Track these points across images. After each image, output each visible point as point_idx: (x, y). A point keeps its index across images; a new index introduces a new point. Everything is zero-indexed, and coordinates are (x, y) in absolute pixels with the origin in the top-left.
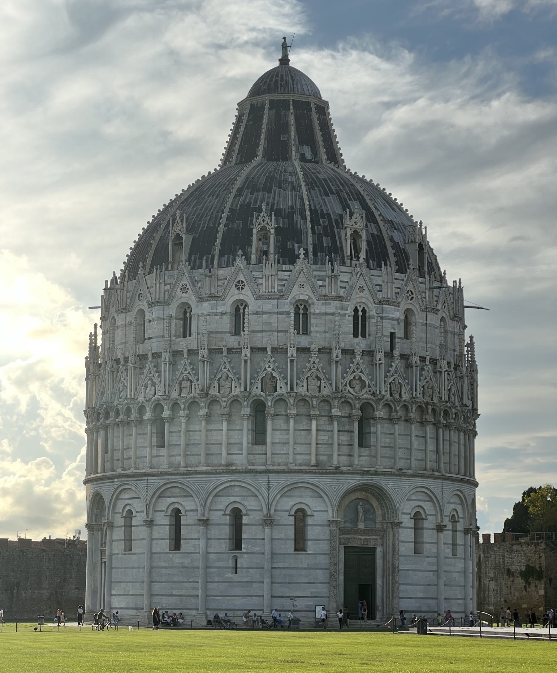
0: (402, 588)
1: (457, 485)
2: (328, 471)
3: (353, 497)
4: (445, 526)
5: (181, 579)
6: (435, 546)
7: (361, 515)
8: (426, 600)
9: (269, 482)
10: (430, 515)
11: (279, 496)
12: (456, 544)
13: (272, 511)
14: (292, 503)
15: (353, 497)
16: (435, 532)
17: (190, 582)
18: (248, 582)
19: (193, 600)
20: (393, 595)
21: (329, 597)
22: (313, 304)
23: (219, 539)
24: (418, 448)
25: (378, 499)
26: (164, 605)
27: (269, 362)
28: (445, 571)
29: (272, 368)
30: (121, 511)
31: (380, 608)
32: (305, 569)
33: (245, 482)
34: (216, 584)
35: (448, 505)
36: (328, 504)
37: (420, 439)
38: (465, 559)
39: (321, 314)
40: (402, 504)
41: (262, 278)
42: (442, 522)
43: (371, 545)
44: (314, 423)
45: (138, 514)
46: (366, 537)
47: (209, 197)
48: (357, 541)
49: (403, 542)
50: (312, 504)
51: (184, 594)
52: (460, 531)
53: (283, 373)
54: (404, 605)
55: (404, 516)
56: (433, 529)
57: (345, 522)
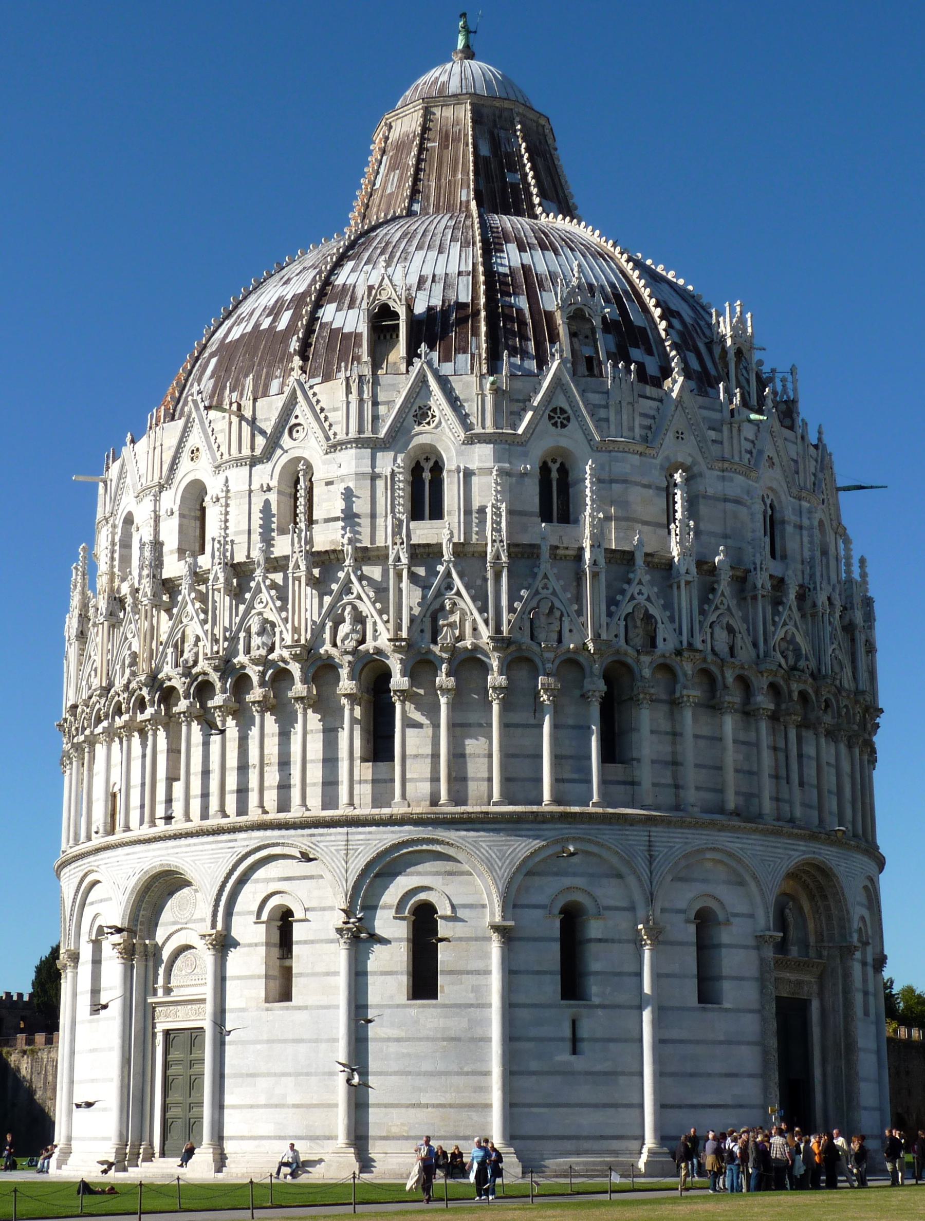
5: (441, 1067)
9: (650, 845)
14: (690, 895)
17: (467, 1074)
18: (606, 1074)
19: (475, 1116)
22: (701, 475)
23: (538, 973)
25: (812, 898)
26: (395, 1130)
27: (640, 583)
29: (645, 596)
30: (255, 908)
33: (598, 844)
34: (534, 1078)
36: (758, 899)
39: (715, 498)
41: (606, 406)
45: (309, 916)
47: (419, 247)
50: (732, 900)
51: (452, 1101)
53: (668, 606)
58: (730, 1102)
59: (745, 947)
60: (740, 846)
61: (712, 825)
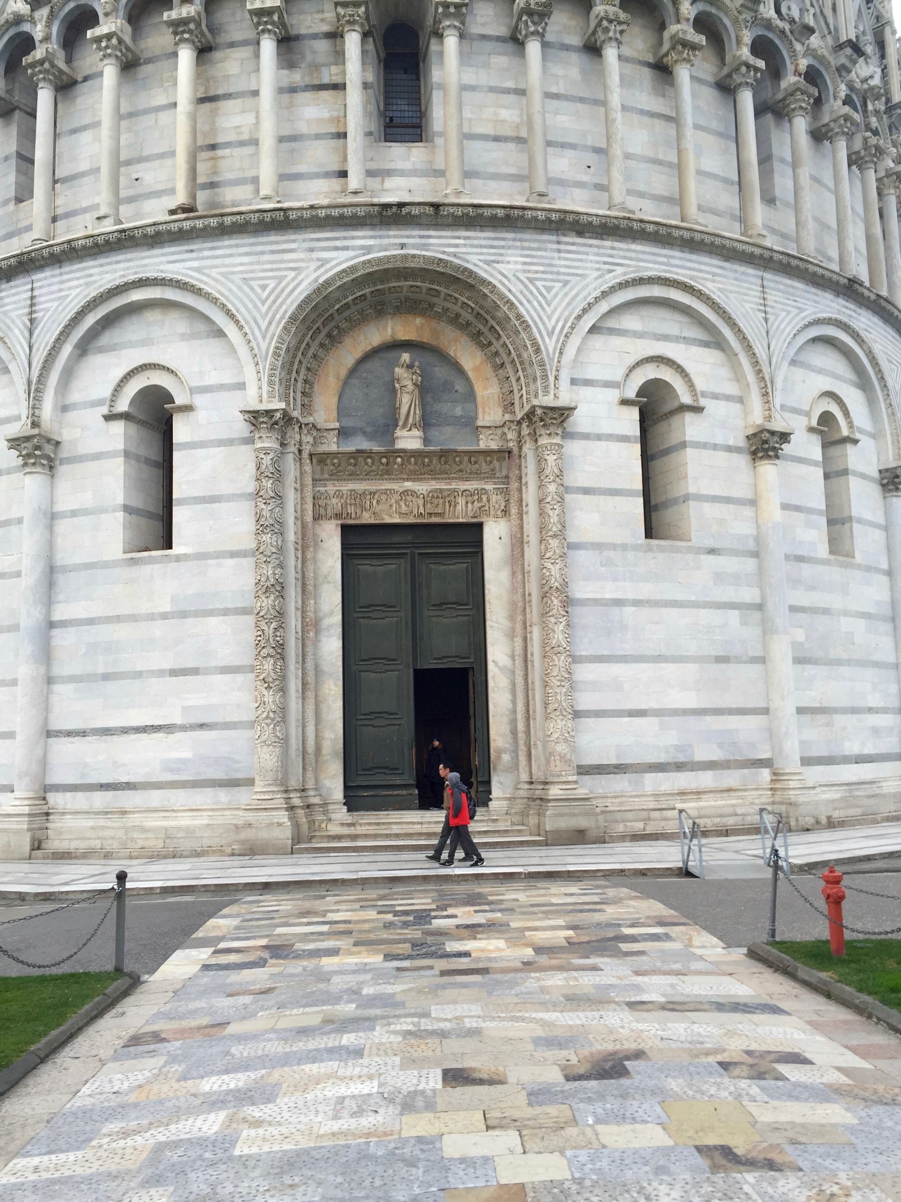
0: (585, 673)
1: (831, 306)
2: (228, 220)
3: (374, 335)
4: (785, 437)
6: (748, 512)
7: (406, 401)
8: (709, 719)
10: (715, 396)
11: (67, 349)
12: (850, 519)
13: (47, 410)
14: (118, 373)
15: (374, 335)
16: (742, 461)
20: (546, 705)
21: (251, 725)
24: (651, 154)
25: (476, 337)
28: (793, 609)
31: (506, 757)
32: (164, 616)
35: (799, 372)
36: (242, 350)
37: (659, 124)
38: (890, 573)
40: (575, 342)
42: (769, 418)
43: (461, 513)
44: (186, 56)
48: (397, 502)
49: (586, 491)
52: (863, 476)
54: (600, 741)
55: (586, 392)
56: (729, 449)
57: (343, 433)
58: (178, 721)
59: (230, 442)
60: (195, 264)
61: (125, 241)
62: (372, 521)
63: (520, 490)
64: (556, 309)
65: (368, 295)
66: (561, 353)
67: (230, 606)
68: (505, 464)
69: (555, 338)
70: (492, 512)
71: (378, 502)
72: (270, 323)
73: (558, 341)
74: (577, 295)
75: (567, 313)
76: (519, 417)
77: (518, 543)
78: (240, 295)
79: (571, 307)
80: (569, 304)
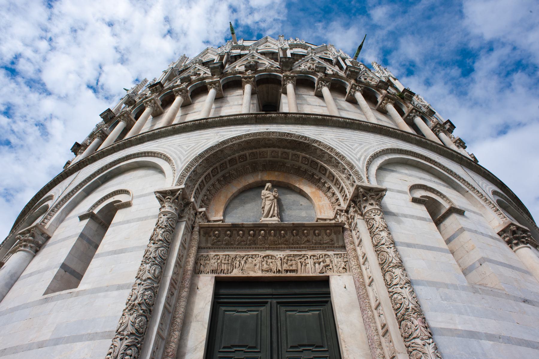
46: (288, 252)
62: (240, 275)
63: (355, 250)
64: (358, 152)
65: (247, 155)
66: (367, 170)
67: (99, 331)
68: (340, 236)
69: (361, 162)
70: (335, 269)
71: (245, 262)
72: (187, 158)
73: (363, 163)
74: (369, 149)
75: (365, 154)
76: (344, 206)
77: (362, 287)
78: (175, 150)
79: (367, 152)
80: (365, 151)
